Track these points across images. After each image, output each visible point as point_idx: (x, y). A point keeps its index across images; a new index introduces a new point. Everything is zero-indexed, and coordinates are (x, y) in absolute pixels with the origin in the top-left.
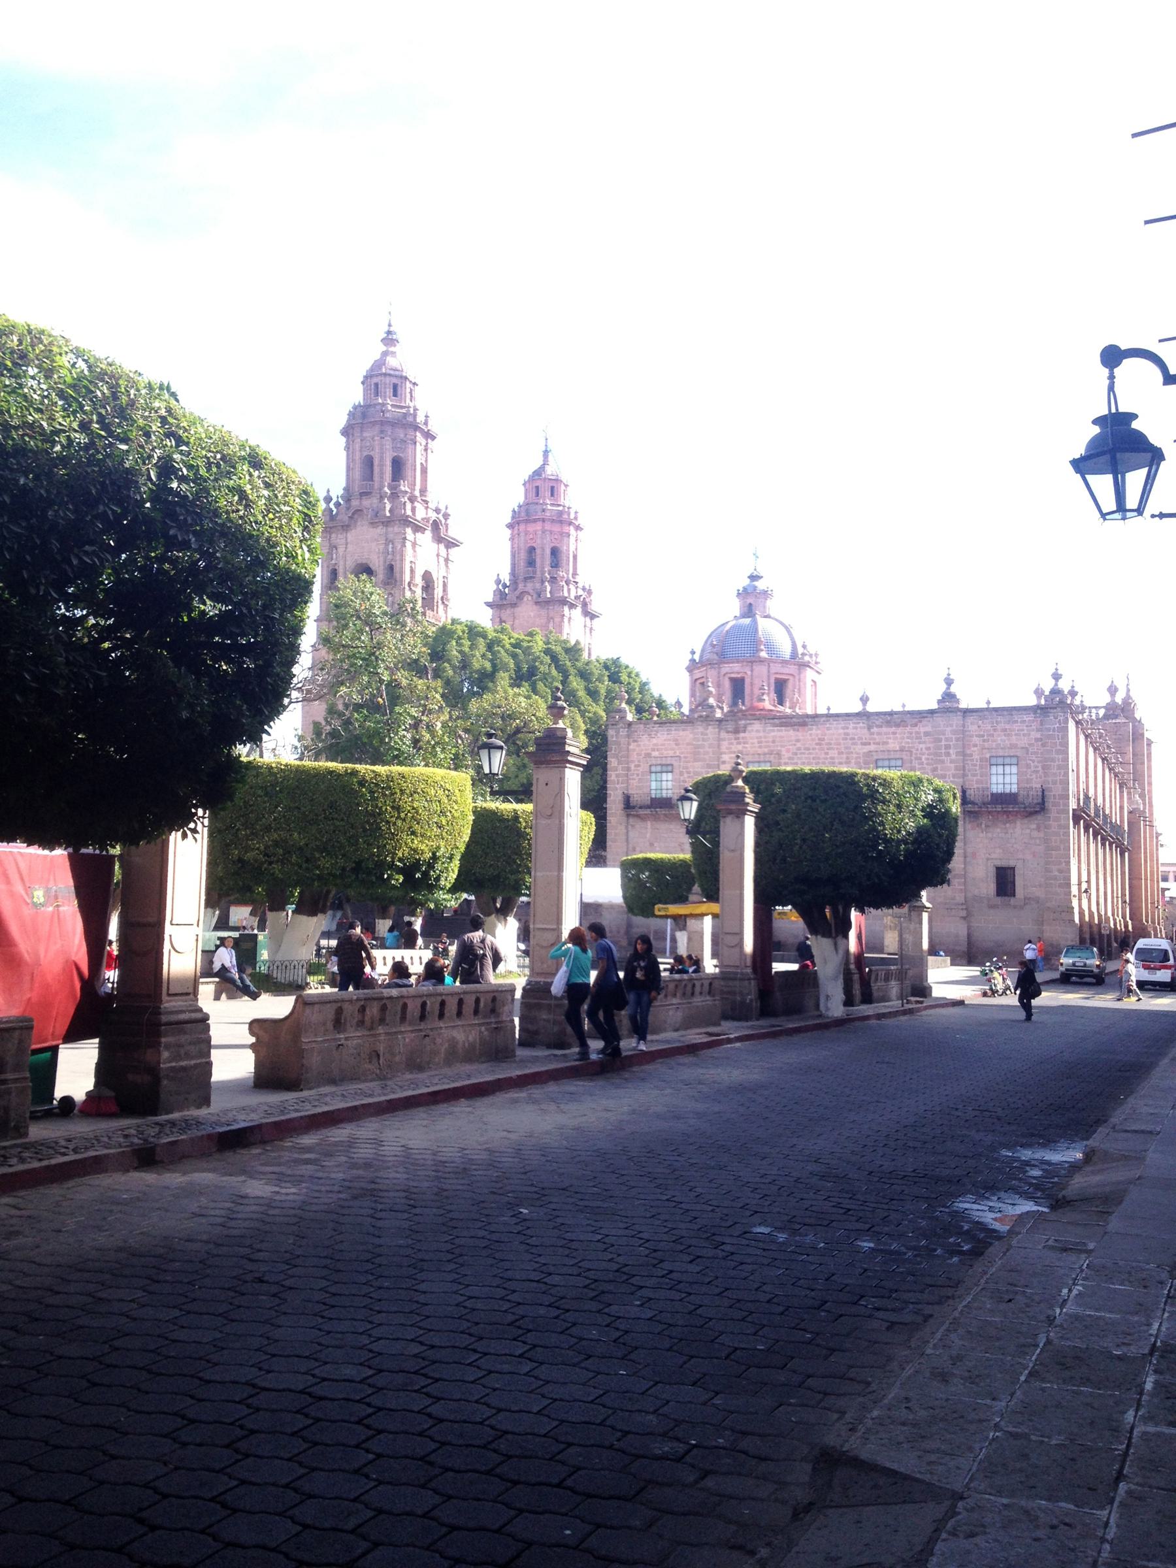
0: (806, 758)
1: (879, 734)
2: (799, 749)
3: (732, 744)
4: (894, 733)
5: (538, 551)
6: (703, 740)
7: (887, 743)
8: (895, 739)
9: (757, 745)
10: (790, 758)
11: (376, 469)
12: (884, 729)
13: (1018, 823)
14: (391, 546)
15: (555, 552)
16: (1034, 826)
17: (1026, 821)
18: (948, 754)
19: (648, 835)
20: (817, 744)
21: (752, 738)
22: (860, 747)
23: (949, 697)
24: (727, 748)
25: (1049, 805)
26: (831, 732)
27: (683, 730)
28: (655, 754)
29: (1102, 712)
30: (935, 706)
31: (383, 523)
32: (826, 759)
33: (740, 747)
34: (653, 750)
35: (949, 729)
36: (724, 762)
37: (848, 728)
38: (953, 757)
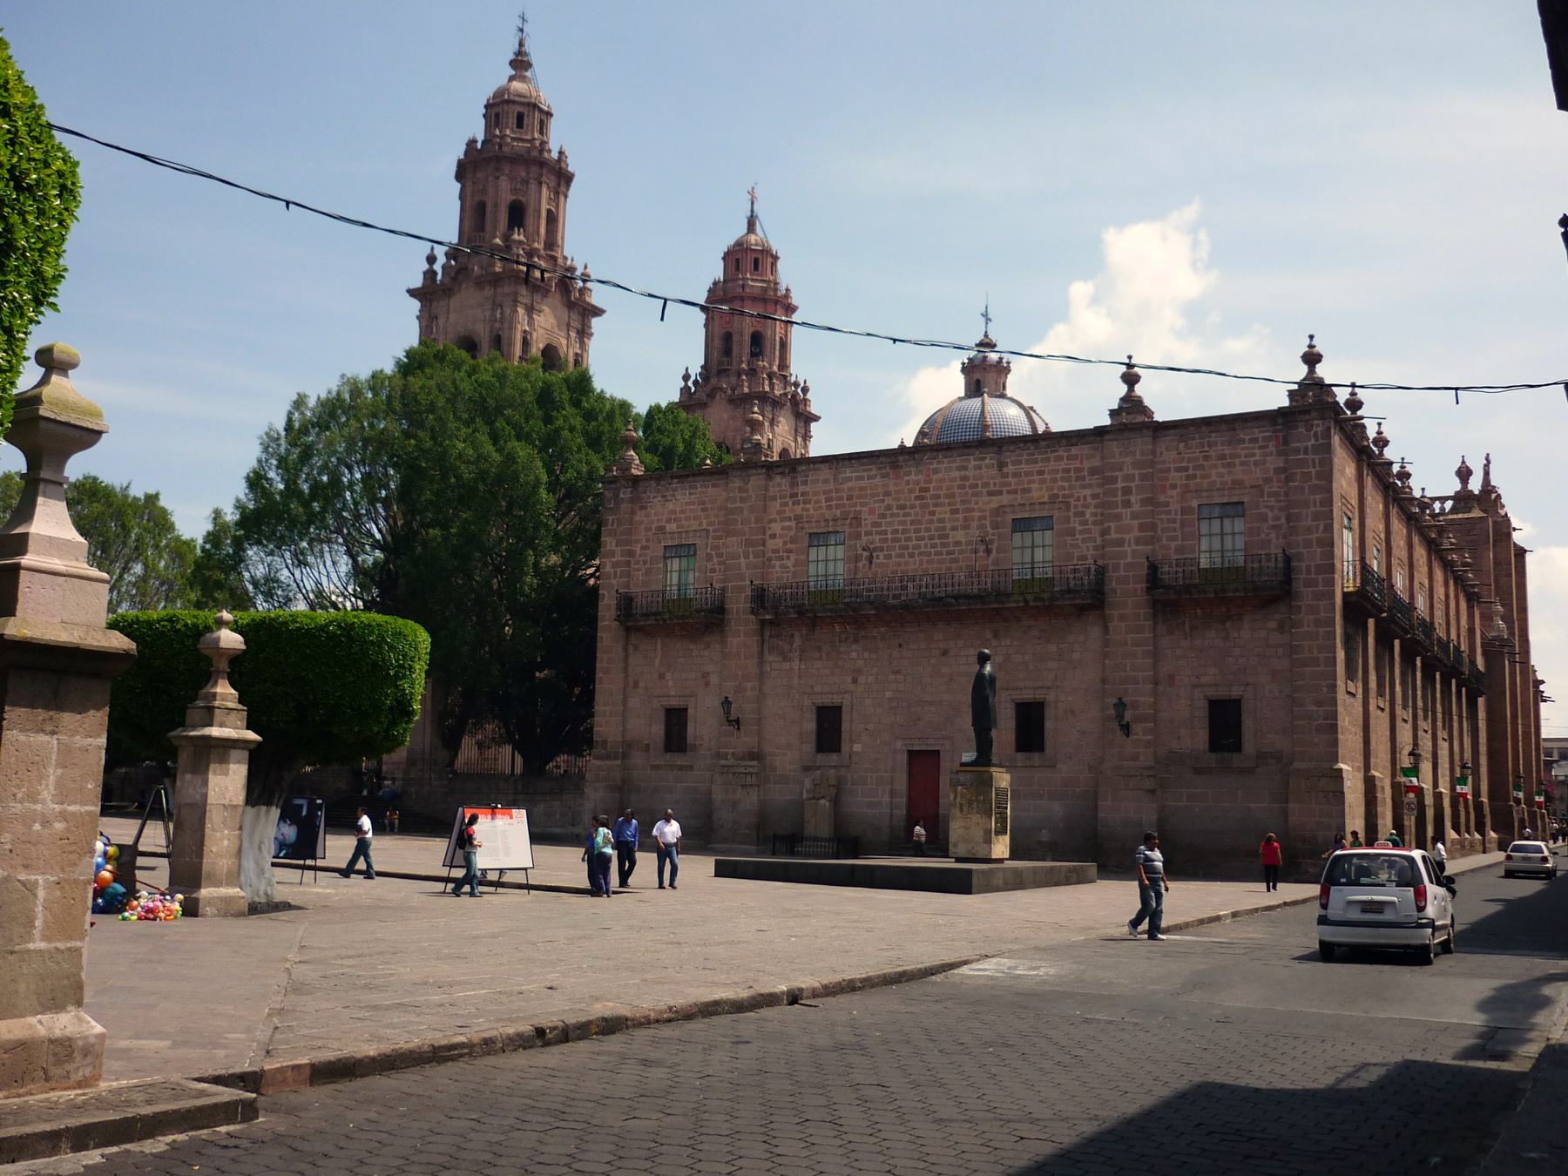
0: (900, 523)
1: (1017, 475)
2: (889, 507)
3: (785, 504)
4: (1041, 473)
5: (735, 338)
6: (742, 500)
7: (1029, 490)
8: (1043, 481)
9: (824, 504)
10: (875, 524)
11: (489, 215)
14: (499, 311)
15: (757, 339)
16: (1272, 625)
18: (1127, 504)
19: (657, 662)
20: (917, 498)
21: (816, 494)
23: (1131, 405)
24: (779, 512)
25: (1299, 584)
26: (940, 476)
27: (714, 485)
28: (672, 527)
29: (1449, 505)
30: (1107, 421)
32: (932, 522)
33: (798, 510)
34: (669, 521)
35: (1129, 460)
36: (773, 536)
37: (965, 468)
38: (1136, 507)
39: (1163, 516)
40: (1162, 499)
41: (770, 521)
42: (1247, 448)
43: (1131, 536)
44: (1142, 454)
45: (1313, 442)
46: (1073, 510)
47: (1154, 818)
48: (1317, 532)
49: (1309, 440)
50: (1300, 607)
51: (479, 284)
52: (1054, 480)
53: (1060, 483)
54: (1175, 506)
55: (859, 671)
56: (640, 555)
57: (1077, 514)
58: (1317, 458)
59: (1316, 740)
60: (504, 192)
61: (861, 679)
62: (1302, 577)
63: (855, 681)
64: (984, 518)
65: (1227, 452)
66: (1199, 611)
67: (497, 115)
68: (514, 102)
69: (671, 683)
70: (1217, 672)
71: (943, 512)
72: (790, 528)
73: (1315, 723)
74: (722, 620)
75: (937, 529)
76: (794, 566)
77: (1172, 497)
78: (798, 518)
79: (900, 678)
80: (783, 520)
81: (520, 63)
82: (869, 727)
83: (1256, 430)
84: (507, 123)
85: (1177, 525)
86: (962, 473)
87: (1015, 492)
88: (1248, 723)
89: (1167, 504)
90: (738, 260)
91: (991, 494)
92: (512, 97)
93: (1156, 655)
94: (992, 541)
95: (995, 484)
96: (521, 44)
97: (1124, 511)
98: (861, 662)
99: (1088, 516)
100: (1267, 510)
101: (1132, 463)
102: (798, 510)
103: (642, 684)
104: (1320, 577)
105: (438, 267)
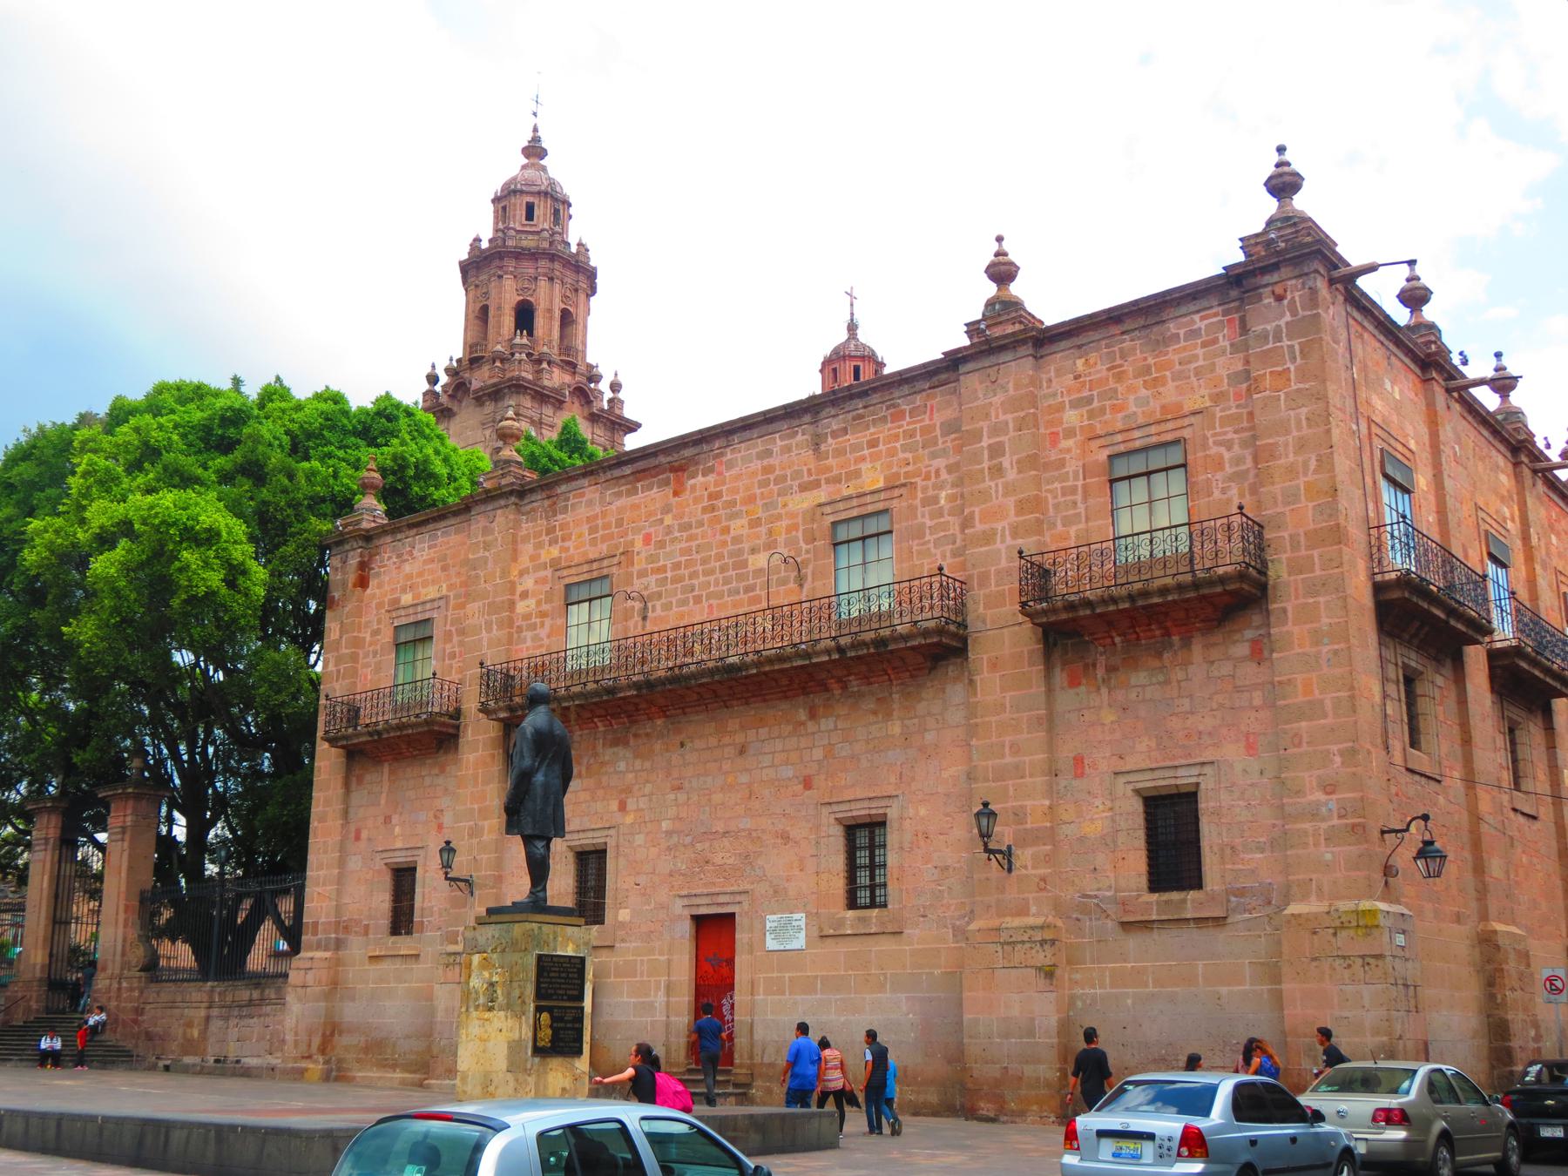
1: (839, 452)
4: (873, 444)
8: (875, 457)
12: (851, 438)
13: (1197, 649)
16: (1242, 650)
17: (1218, 637)
18: (998, 471)
20: (704, 510)
22: (797, 497)
23: (1004, 308)
25: (1279, 571)
28: (407, 599)
30: (966, 342)
31: (489, 395)
32: (724, 543)
34: (404, 590)
35: (997, 399)
38: (1011, 475)
39: (1057, 485)
40: (1053, 456)
41: (521, 574)
42: (1185, 348)
43: (1005, 523)
44: (1017, 388)
45: (1288, 317)
46: (920, 495)
47: (1053, 1021)
48: (1305, 474)
49: (1282, 315)
50: (1284, 611)
51: (479, 400)
52: (892, 453)
53: (901, 455)
54: (1072, 466)
55: (628, 790)
56: (370, 645)
57: (927, 502)
58: (1296, 343)
59: (1328, 856)
60: (508, 294)
61: (631, 805)
62: (1284, 556)
63: (623, 807)
64: (795, 527)
65: (1151, 361)
66: (1117, 640)
67: (504, 208)
68: (522, 192)
69: (397, 830)
70: (1153, 745)
71: (739, 526)
72: (544, 581)
73: (1324, 825)
74: (458, 727)
75: (731, 555)
76: (548, 637)
77: (1069, 450)
78: (556, 565)
79: (682, 797)
80: (537, 568)
81: (535, 151)
82: (642, 879)
83: (1196, 317)
84: (514, 216)
85: (1079, 497)
86: (765, 462)
87: (837, 480)
88: (1210, 835)
89: (1062, 463)
90: (835, 370)
91: (804, 488)
92: (519, 186)
93: (1050, 722)
94: (806, 562)
95: (810, 472)
96: (535, 130)
97: (992, 484)
98: (631, 776)
99: (943, 502)
100: (1222, 450)
101: (1002, 404)
102: (555, 552)
103: (364, 835)
104: (1316, 553)
105: (438, 388)
